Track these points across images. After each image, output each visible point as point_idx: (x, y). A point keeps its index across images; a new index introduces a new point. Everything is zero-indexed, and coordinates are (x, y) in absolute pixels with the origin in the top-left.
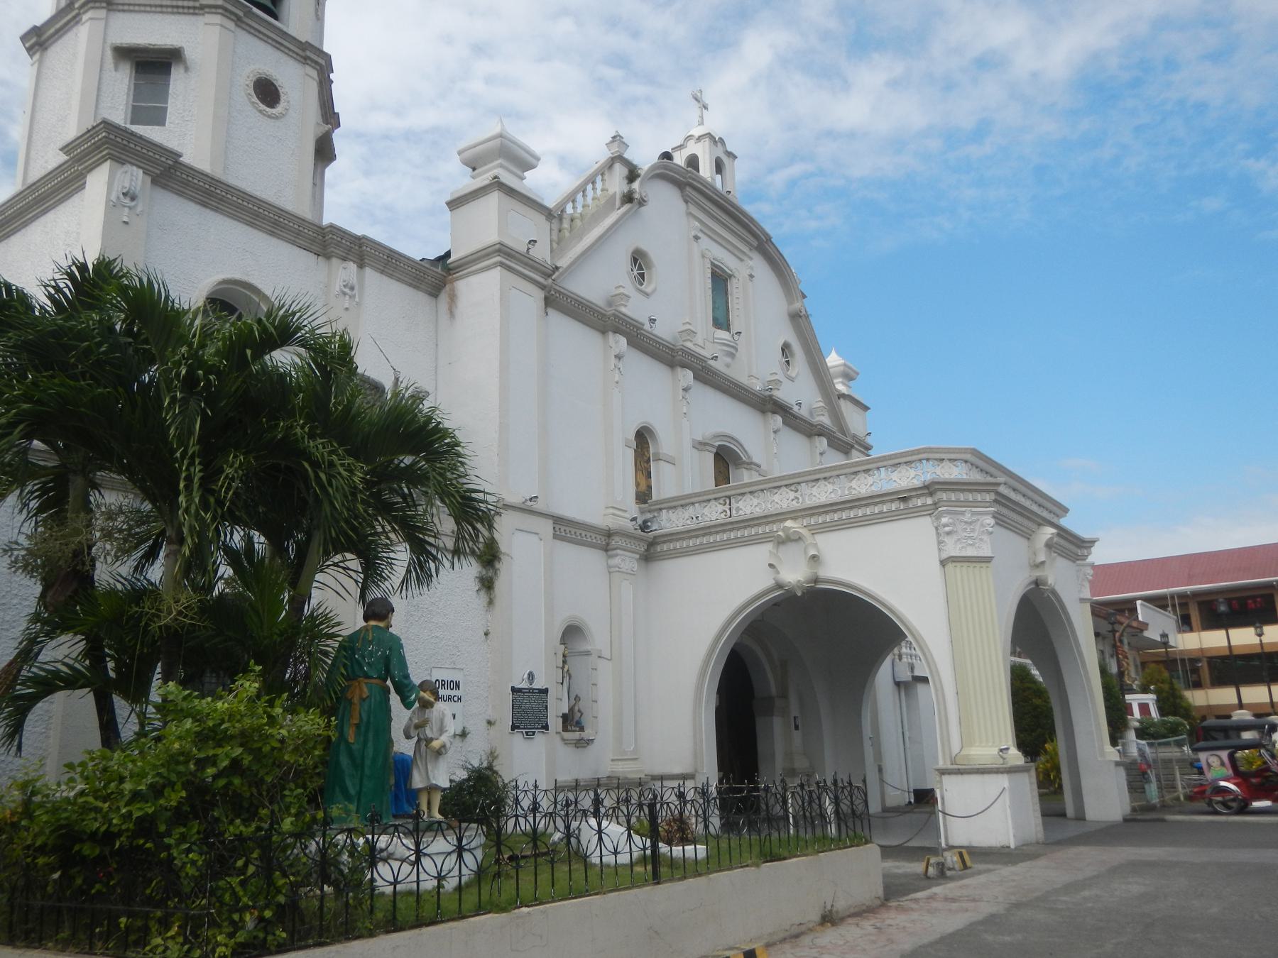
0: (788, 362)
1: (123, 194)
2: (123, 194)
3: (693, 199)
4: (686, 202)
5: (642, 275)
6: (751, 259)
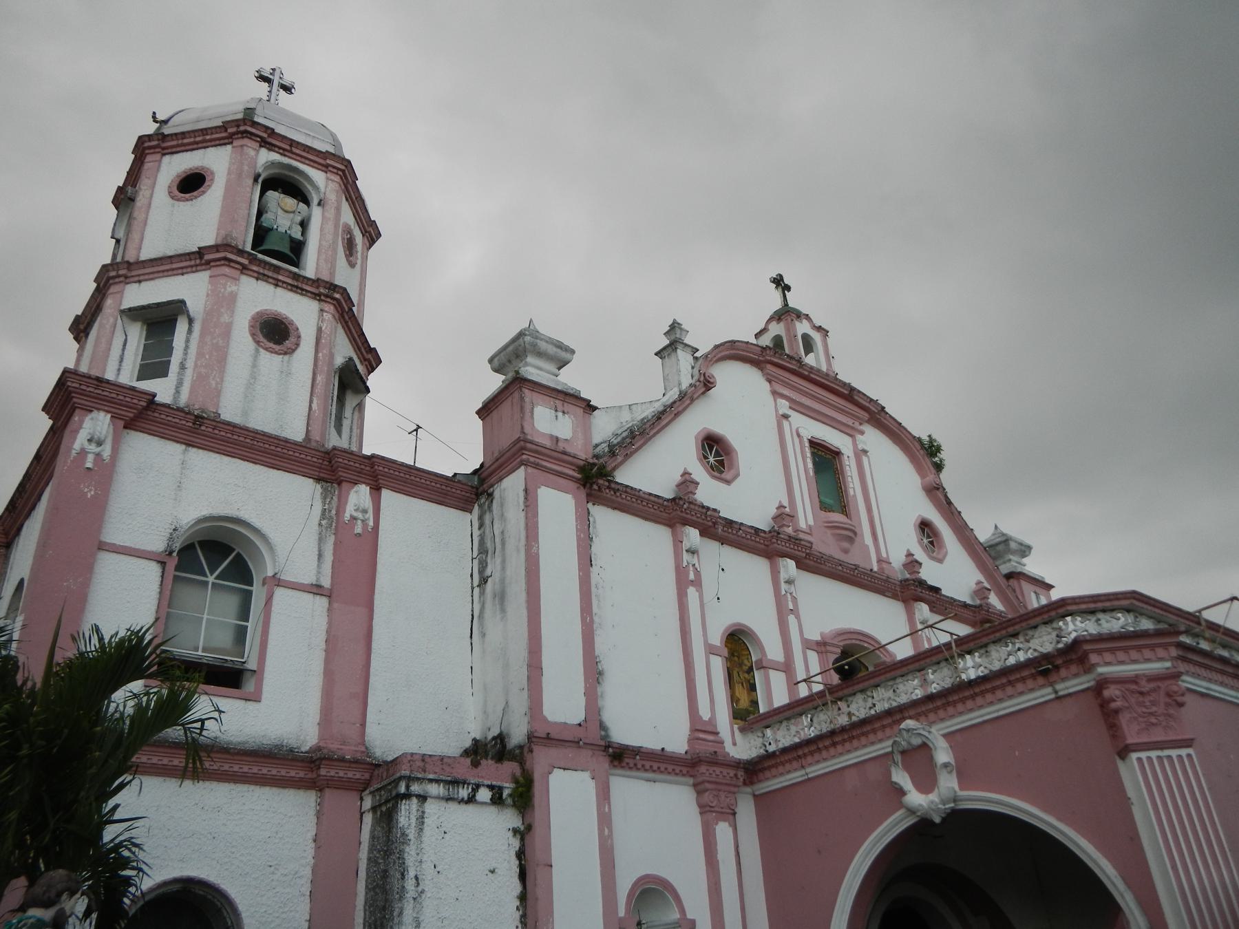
0: (931, 543)
1: (88, 440)
2: (88, 440)
3: (774, 377)
4: (770, 381)
5: (721, 463)
6: (862, 433)
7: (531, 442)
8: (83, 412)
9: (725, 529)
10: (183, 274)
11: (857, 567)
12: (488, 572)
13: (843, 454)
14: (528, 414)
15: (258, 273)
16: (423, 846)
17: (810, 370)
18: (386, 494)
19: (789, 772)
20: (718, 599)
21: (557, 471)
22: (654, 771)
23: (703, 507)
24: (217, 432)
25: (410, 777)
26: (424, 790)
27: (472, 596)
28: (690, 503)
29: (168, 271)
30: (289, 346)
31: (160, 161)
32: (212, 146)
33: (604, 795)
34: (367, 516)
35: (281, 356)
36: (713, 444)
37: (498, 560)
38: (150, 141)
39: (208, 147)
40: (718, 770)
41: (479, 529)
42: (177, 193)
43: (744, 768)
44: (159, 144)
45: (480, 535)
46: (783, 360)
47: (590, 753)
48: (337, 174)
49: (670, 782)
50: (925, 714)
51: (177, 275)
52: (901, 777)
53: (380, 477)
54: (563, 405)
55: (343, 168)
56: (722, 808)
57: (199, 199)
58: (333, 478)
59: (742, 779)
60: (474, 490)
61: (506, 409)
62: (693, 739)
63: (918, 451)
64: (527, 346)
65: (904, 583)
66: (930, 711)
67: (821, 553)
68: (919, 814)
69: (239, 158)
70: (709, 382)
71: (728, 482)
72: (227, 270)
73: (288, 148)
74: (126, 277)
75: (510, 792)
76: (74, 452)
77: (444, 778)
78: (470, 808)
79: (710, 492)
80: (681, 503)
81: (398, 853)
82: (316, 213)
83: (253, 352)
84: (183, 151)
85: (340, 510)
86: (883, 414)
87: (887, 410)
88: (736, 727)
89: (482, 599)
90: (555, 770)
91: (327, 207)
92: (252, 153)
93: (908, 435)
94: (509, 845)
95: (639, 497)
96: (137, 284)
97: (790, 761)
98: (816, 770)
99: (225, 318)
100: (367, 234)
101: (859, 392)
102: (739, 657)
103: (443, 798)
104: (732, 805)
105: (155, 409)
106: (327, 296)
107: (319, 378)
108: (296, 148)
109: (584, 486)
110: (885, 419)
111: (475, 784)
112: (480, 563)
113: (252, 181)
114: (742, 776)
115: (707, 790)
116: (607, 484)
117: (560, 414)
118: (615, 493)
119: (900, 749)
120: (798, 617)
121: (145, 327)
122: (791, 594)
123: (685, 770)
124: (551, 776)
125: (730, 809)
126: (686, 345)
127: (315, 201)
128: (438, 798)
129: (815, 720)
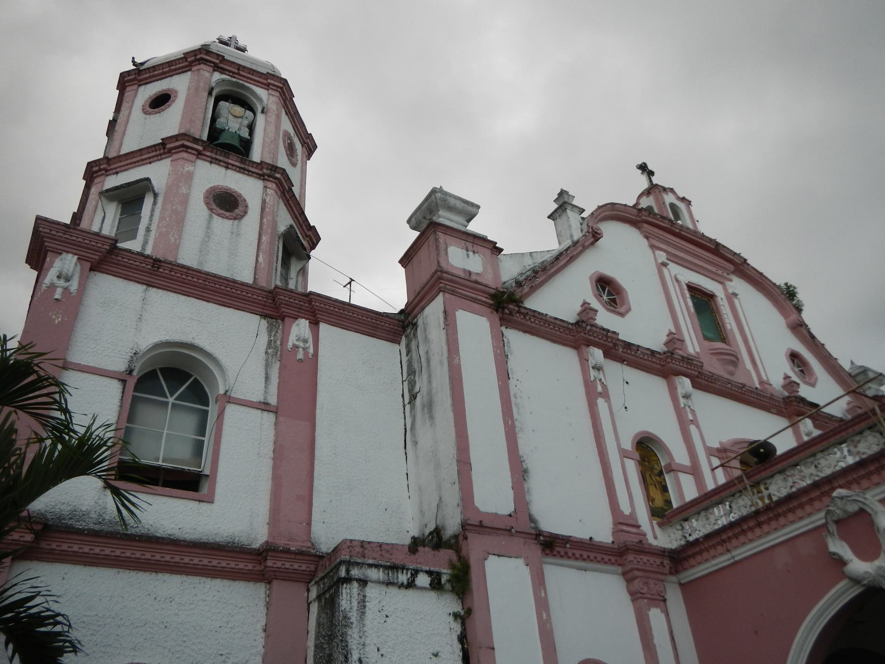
0: (802, 371)
4: (647, 238)
5: (614, 301)
6: (731, 280)
7: (447, 273)
8: (54, 254)
9: (625, 350)
10: (150, 163)
11: (744, 386)
12: (417, 389)
13: (717, 296)
14: (442, 253)
15: (212, 158)
16: (366, 629)
17: (680, 228)
18: (324, 327)
19: (714, 557)
20: (626, 408)
21: (470, 297)
22: (584, 560)
23: (604, 329)
24: (173, 273)
25: (349, 561)
26: (364, 575)
27: (404, 413)
28: (592, 325)
29: (138, 161)
30: (238, 213)
31: (137, 90)
32: (177, 74)
33: (539, 582)
34: (307, 345)
35: (231, 221)
36: (605, 285)
37: (425, 376)
38: (129, 76)
39: (173, 75)
40: (645, 558)
41: (407, 355)
42: (149, 109)
43: (670, 557)
44: (136, 77)
45: (408, 360)
46: (657, 219)
47: (522, 541)
48: (277, 90)
49: (602, 571)
50: (857, 481)
51: (146, 164)
52: (838, 547)
53: (317, 312)
54: (473, 246)
55: (281, 85)
56: (652, 595)
57: (166, 111)
58: (278, 314)
59: (668, 568)
60: (401, 323)
61: (423, 253)
62: (617, 532)
63: (780, 295)
64: (438, 201)
65: (787, 401)
66: (862, 477)
67: (710, 372)
68: (865, 582)
69: (197, 78)
70: (596, 233)
71: (622, 315)
72: (185, 155)
73: (236, 71)
74: (107, 171)
75: (448, 578)
76: (44, 285)
77: (383, 563)
78: (410, 593)
79: (605, 319)
80: (584, 325)
81: (341, 635)
82: (261, 119)
83: (207, 217)
84: (154, 81)
85: (284, 340)
86: (746, 265)
87: (748, 262)
88: (654, 522)
89: (413, 413)
90: (491, 556)
91: (269, 114)
92: (207, 74)
93: (769, 283)
94: (450, 629)
95: (546, 321)
96: (115, 175)
97: (714, 547)
98: (742, 552)
99: (183, 190)
100: (306, 145)
101: (724, 247)
102: (649, 462)
103: (383, 583)
104: (662, 592)
105: (118, 254)
106: (269, 176)
107: (264, 238)
108: (243, 71)
109: (497, 311)
110: (748, 269)
111: (414, 570)
112: (410, 383)
113: (207, 93)
114: (667, 564)
115: (636, 578)
116: (517, 309)
117: (471, 253)
118: (525, 317)
119: (835, 518)
120: (698, 427)
121: (120, 206)
122: (689, 407)
123: (613, 559)
124: (486, 562)
125: (661, 596)
126: (574, 206)
127: (260, 110)
128: (378, 582)
129: (733, 505)
